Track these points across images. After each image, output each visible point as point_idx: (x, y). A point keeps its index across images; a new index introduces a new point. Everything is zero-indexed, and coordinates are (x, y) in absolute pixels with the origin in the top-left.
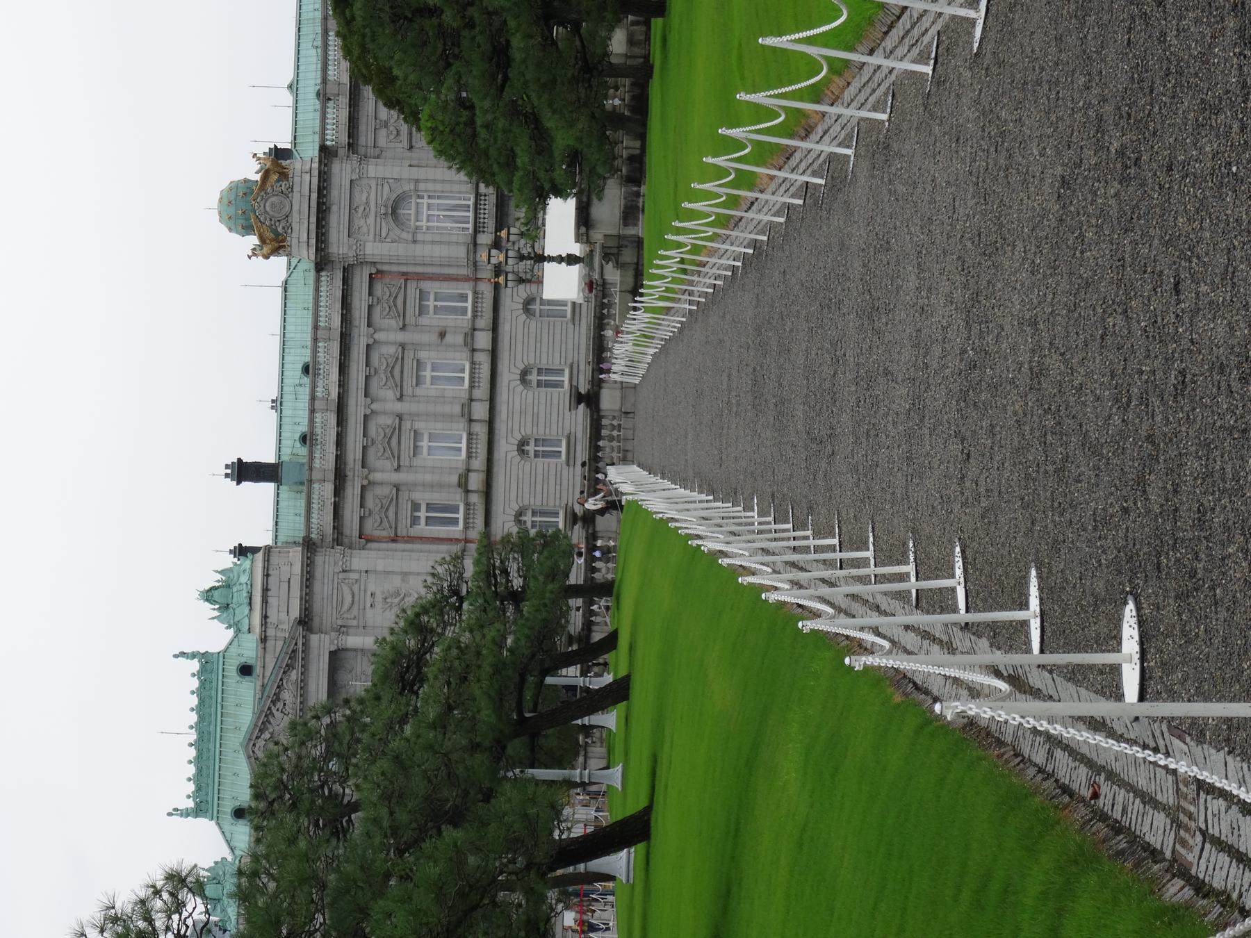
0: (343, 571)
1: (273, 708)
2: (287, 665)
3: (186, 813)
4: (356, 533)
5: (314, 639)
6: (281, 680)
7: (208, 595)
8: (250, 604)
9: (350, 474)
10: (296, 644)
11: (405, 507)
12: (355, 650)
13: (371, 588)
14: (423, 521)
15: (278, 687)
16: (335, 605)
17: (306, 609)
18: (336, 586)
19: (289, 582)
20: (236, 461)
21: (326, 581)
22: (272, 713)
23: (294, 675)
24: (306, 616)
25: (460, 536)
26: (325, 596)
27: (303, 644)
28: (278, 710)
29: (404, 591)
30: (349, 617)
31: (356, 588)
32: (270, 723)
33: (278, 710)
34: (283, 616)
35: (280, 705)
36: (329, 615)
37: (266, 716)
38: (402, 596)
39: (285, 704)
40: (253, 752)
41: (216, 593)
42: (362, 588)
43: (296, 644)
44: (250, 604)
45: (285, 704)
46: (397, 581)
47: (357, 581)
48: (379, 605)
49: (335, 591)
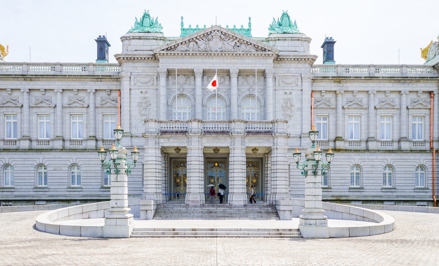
1: (236, 41)
2: (258, 46)
6: (251, 44)
10: (269, 51)
12: (265, 85)
15: (247, 42)
17: (284, 59)
19: (295, 51)
20: (335, 41)
22: (234, 40)
23: (253, 50)
24: (280, 59)
27: (269, 55)
28: (236, 43)
30: (280, 82)
32: (229, 40)
33: (236, 43)
35: (238, 44)
36: (281, 72)
37: (233, 36)
39: (238, 46)
42: (294, 88)
43: (269, 51)
48: (286, 97)
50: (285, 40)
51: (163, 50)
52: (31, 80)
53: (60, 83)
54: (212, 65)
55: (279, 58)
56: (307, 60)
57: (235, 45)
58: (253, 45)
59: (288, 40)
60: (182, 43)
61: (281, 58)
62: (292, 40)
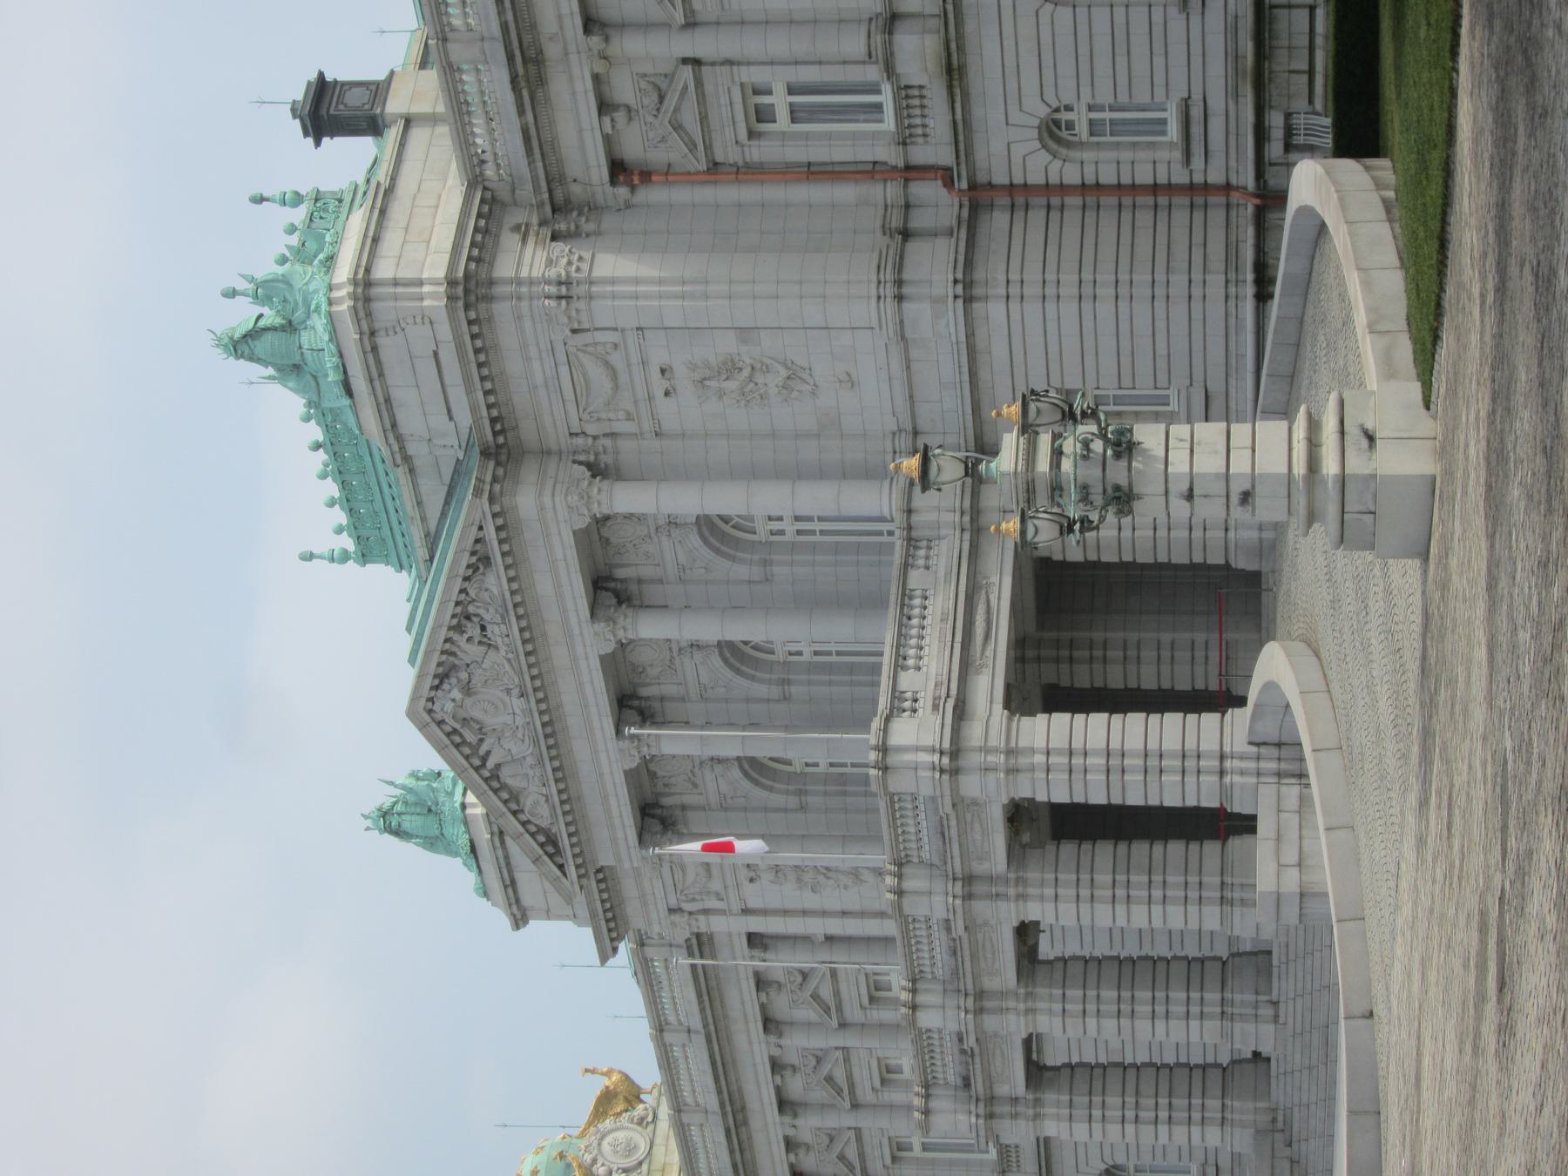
0: (574, 331)
3: (345, 557)
4: (599, 171)
5: (526, 501)
6: (463, 591)
7: (242, 345)
8: (349, 392)
9: (552, 51)
11: (724, 100)
13: (658, 357)
14: (782, 114)
16: (569, 394)
18: (562, 358)
21: (533, 352)
23: (495, 582)
25: (888, 154)
26: (539, 379)
28: (469, 639)
29: (748, 361)
31: (616, 358)
33: (469, 639)
34: (439, 420)
35: (473, 630)
38: (746, 372)
39: (483, 628)
40: (430, 712)
41: (261, 346)
44: (349, 392)
45: (483, 628)
46: (728, 344)
47: (616, 346)
49: (564, 370)
50: (388, 400)
51: (561, 867)
52: (743, 1109)
53: (740, 1040)
54: (593, 710)
55: (491, 443)
56: (479, 343)
57: (480, 643)
58: (466, 584)
59: (385, 388)
60: (515, 813)
61: (490, 437)
62: (381, 375)
